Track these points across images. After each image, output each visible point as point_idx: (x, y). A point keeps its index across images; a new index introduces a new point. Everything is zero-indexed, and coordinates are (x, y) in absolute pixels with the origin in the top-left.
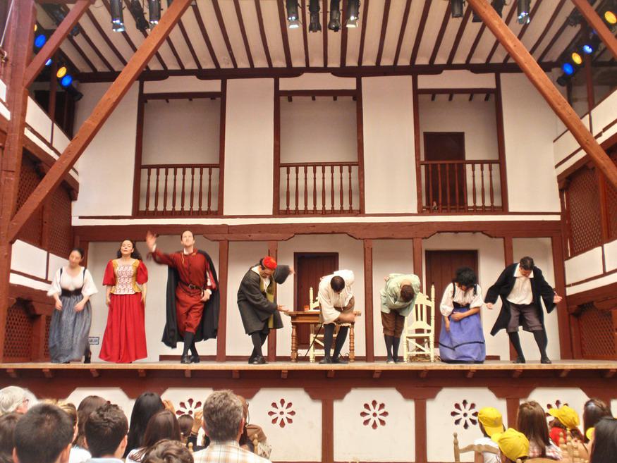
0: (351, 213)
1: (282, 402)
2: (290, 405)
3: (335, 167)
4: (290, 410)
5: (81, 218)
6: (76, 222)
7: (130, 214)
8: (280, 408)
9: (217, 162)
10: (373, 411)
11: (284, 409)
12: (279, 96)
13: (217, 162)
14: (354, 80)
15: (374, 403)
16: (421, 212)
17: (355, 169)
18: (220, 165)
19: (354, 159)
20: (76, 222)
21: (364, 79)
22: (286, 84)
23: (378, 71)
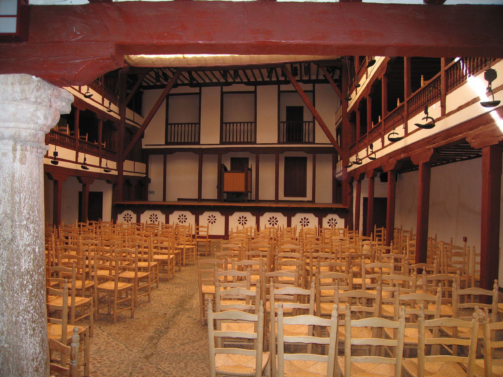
0: (251, 143)
1: (212, 216)
2: (214, 217)
3: (249, 124)
4: (215, 218)
5: (145, 145)
7: (164, 143)
8: (212, 218)
9: (198, 122)
10: (242, 219)
11: (212, 218)
12: (223, 93)
14: (253, 87)
15: (243, 217)
17: (253, 124)
18: (199, 123)
19: (253, 120)
21: (257, 87)
22: (226, 89)
23: (264, 83)
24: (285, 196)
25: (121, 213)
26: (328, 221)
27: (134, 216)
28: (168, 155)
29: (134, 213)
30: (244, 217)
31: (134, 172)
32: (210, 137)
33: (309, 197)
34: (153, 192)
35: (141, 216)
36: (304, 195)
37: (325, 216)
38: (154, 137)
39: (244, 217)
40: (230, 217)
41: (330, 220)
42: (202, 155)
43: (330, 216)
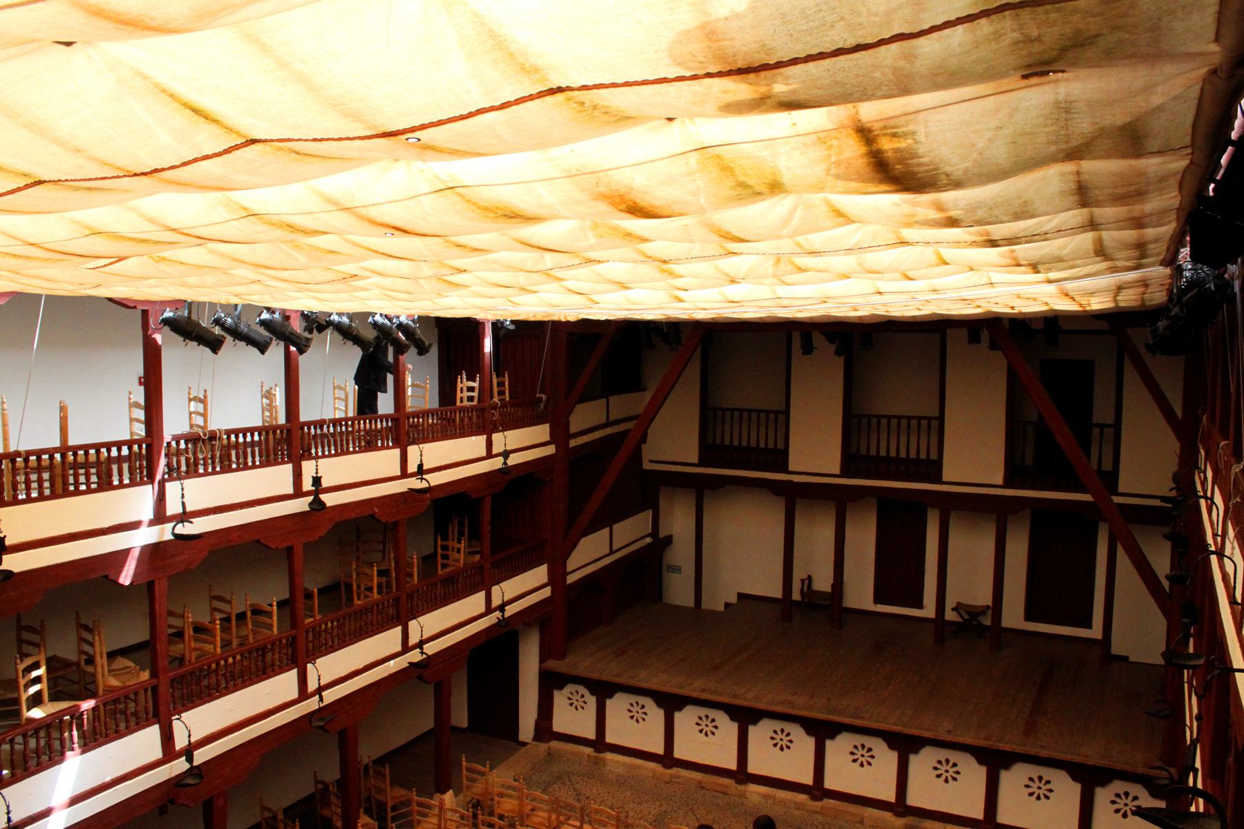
1: (782, 731)
2: (788, 734)
5: (651, 461)
6: (647, 466)
11: (783, 737)
13: (783, 408)
16: (1008, 483)
17: (935, 423)
18: (787, 413)
20: (647, 466)
24: (1028, 617)
25: (561, 688)
26: (1114, 798)
27: (592, 701)
28: (706, 492)
29: (592, 694)
30: (867, 746)
31: (612, 552)
32: (816, 451)
33: (1096, 632)
34: (677, 569)
35: (609, 702)
36: (1088, 625)
37: (1104, 783)
38: (674, 442)
39: (867, 746)
40: (828, 743)
41: (1118, 795)
42: (796, 497)
43: (1118, 786)
